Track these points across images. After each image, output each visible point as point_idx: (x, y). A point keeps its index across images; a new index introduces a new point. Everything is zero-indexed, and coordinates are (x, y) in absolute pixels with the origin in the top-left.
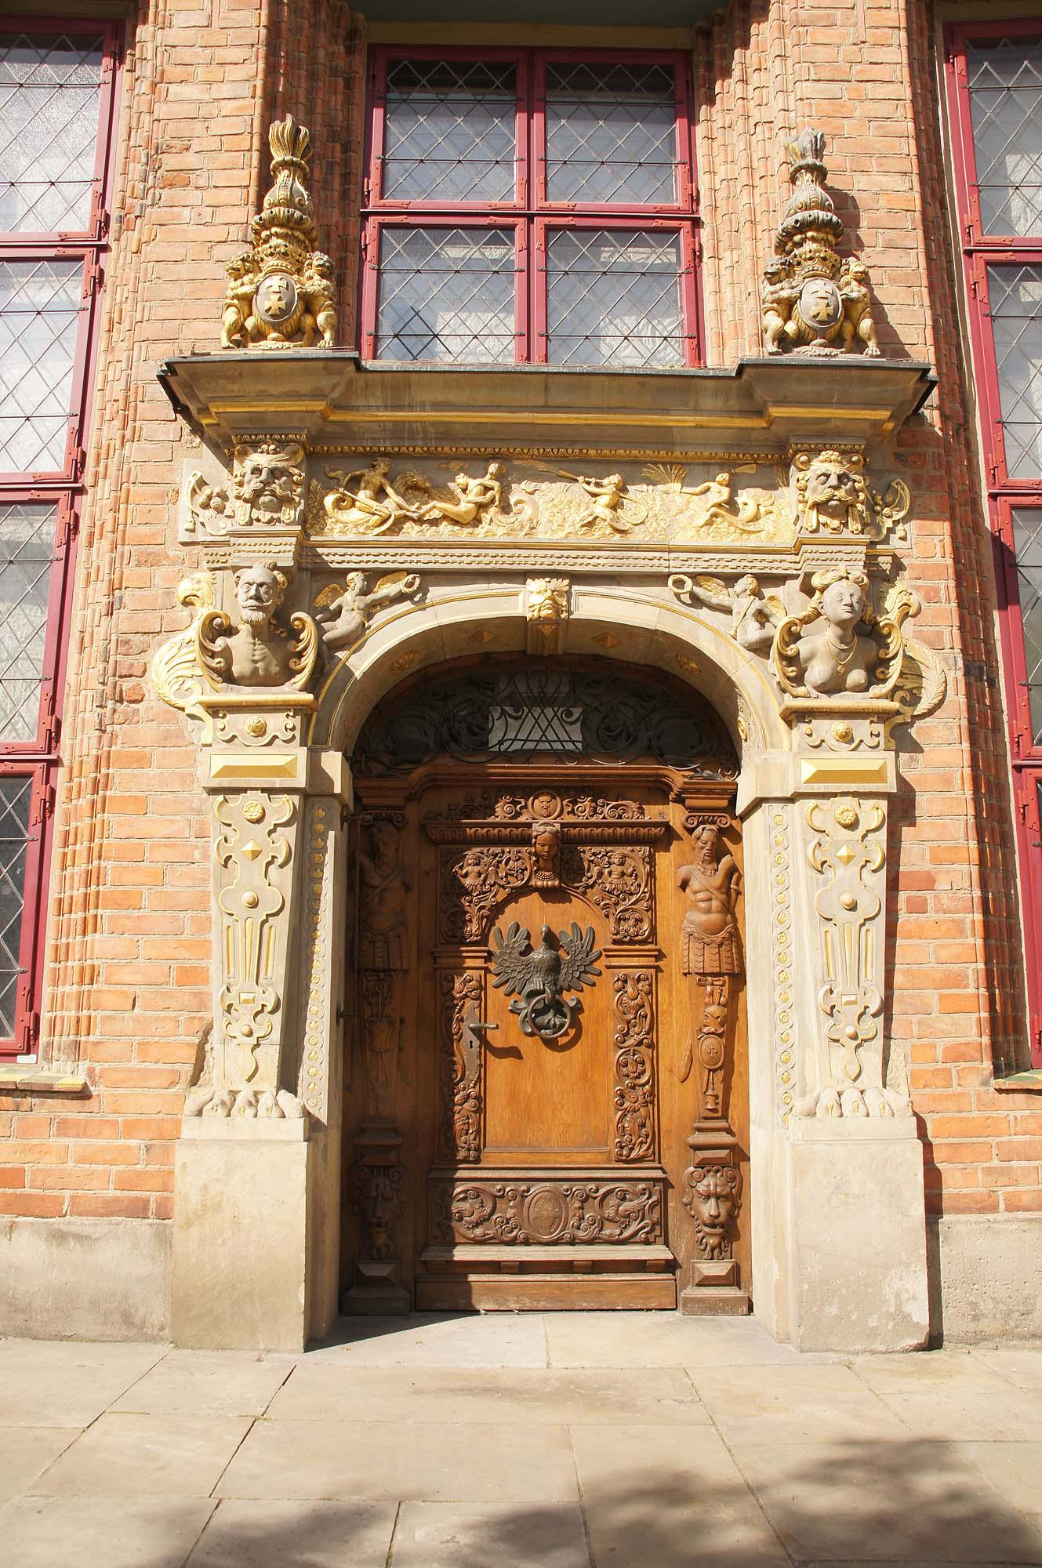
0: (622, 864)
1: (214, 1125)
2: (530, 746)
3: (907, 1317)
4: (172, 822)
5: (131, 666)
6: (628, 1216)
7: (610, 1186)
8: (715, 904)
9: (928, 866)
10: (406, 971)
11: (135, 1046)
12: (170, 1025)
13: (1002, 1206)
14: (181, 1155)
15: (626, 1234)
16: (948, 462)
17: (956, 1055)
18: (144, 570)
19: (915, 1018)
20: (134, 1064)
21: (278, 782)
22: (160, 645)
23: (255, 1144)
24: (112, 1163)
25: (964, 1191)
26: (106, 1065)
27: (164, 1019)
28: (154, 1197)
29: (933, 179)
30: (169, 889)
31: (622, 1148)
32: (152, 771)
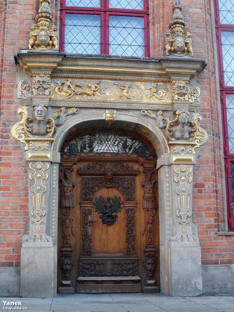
0: (128, 181)
1: (31, 244)
2: (105, 151)
3: (197, 288)
4: (18, 169)
5: (6, 130)
6: (129, 269)
7: (125, 261)
8: (151, 191)
9: (202, 182)
10: (73, 207)
11: (9, 225)
12: (18, 219)
13: (220, 263)
14: (23, 251)
15: (129, 274)
16: (210, 83)
17: (209, 227)
18: (9, 105)
19: (199, 218)
20: (9, 229)
21: (45, 160)
22: (13, 124)
23: (41, 248)
24: (4, 253)
25: (211, 259)
26: (2, 229)
27: (16, 218)
28: (14, 261)
29: (208, 9)
30: (17, 186)
31: (128, 252)
32: (12, 156)
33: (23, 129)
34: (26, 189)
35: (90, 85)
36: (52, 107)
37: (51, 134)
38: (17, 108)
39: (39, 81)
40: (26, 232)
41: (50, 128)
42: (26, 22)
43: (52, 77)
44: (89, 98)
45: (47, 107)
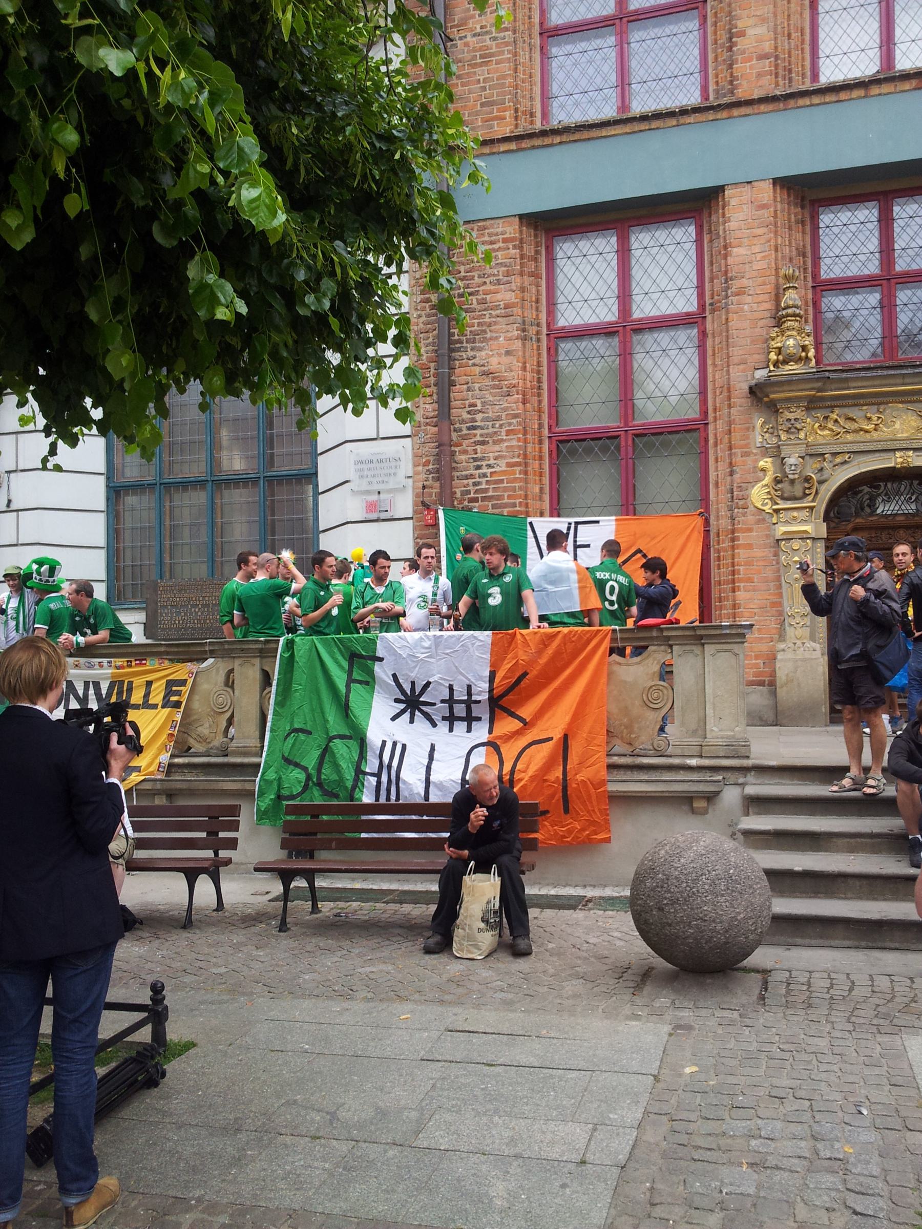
1: (789, 655)
2: (895, 512)
14: (778, 665)
22: (753, 487)
32: (755, 534)
33: (769, 493)
34: (778, 579)
35: (868, 415)
36: (811, 455)
37: (811, 498)
38: (757, 461)
39: (789, 420)
40: (782, 637)
41: (809, 488)
42: (761, 323)
43: (808, 409)
44: (868, 436)
45: (803, 458)
